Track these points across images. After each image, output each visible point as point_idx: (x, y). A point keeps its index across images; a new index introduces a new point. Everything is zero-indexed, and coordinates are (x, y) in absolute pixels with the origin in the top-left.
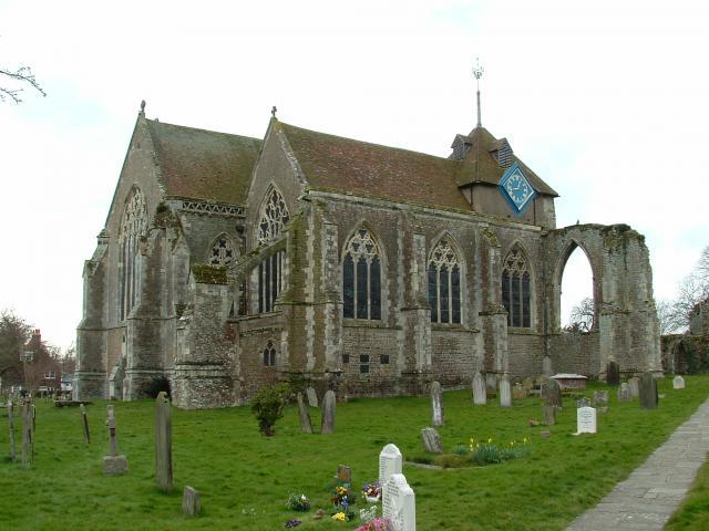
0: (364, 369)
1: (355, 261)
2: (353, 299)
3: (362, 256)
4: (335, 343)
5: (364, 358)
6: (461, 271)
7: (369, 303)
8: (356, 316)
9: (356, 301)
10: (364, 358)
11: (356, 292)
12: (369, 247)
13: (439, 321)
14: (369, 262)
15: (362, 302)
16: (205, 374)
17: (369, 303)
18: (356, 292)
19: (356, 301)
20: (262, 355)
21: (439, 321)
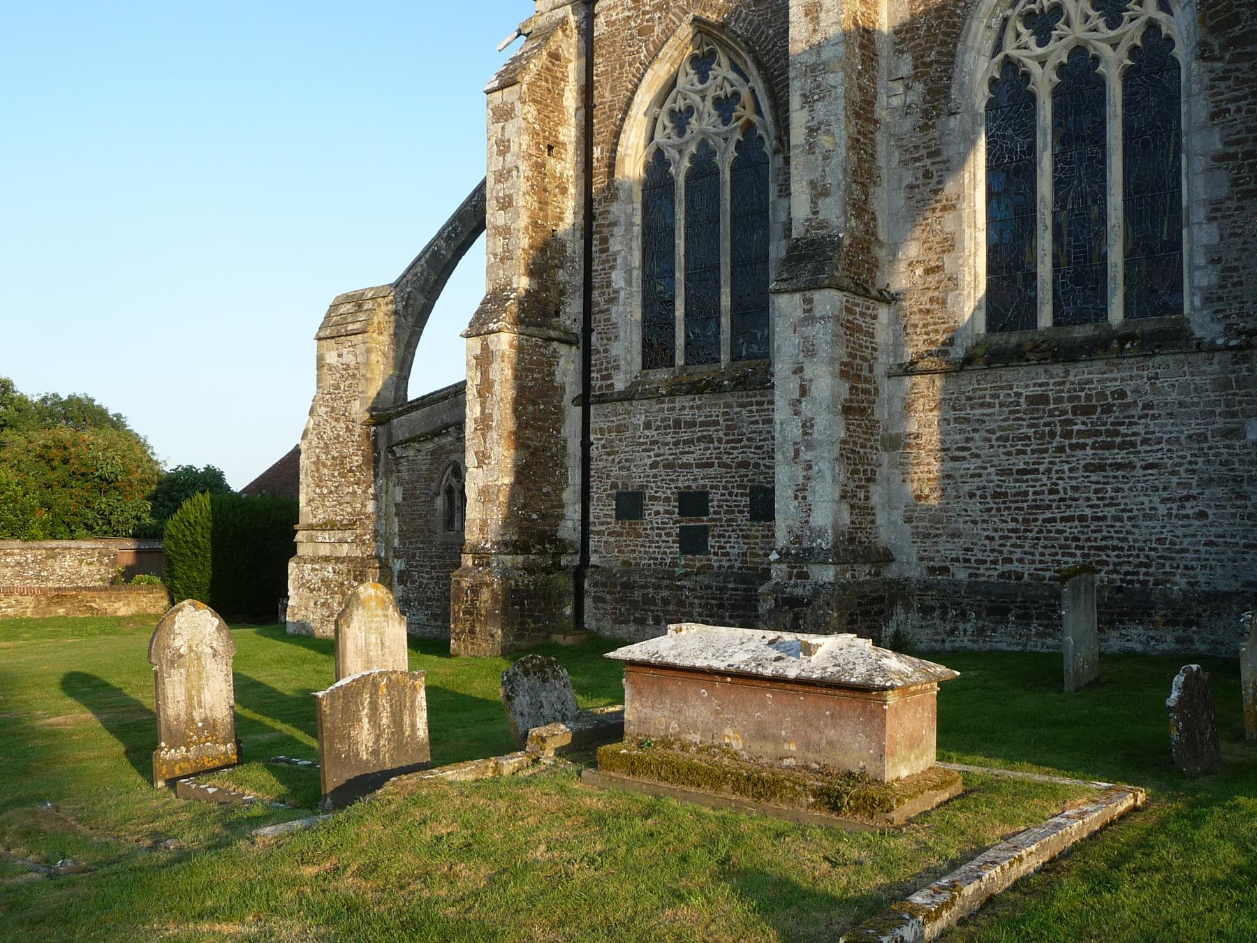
0: (692, 541)
1: (681, 169)
2: (672, 302)
3: (703, 144)
4: (483, 458)
5: (692, 502)
6: (1181, 52)
7: (726, 301)
8: (680, 360)
9: (680, 311)
10: (692, 502)
11: (680, 276)
12: (725, 106)
13: (1045, 319)
14: (725, 160)
15: (703, 312)
16: (325, 550)
17: (726, 301)
18: (680, 276)
19: (680, 311)
20: (440, 502)
21: (1045, 319)
